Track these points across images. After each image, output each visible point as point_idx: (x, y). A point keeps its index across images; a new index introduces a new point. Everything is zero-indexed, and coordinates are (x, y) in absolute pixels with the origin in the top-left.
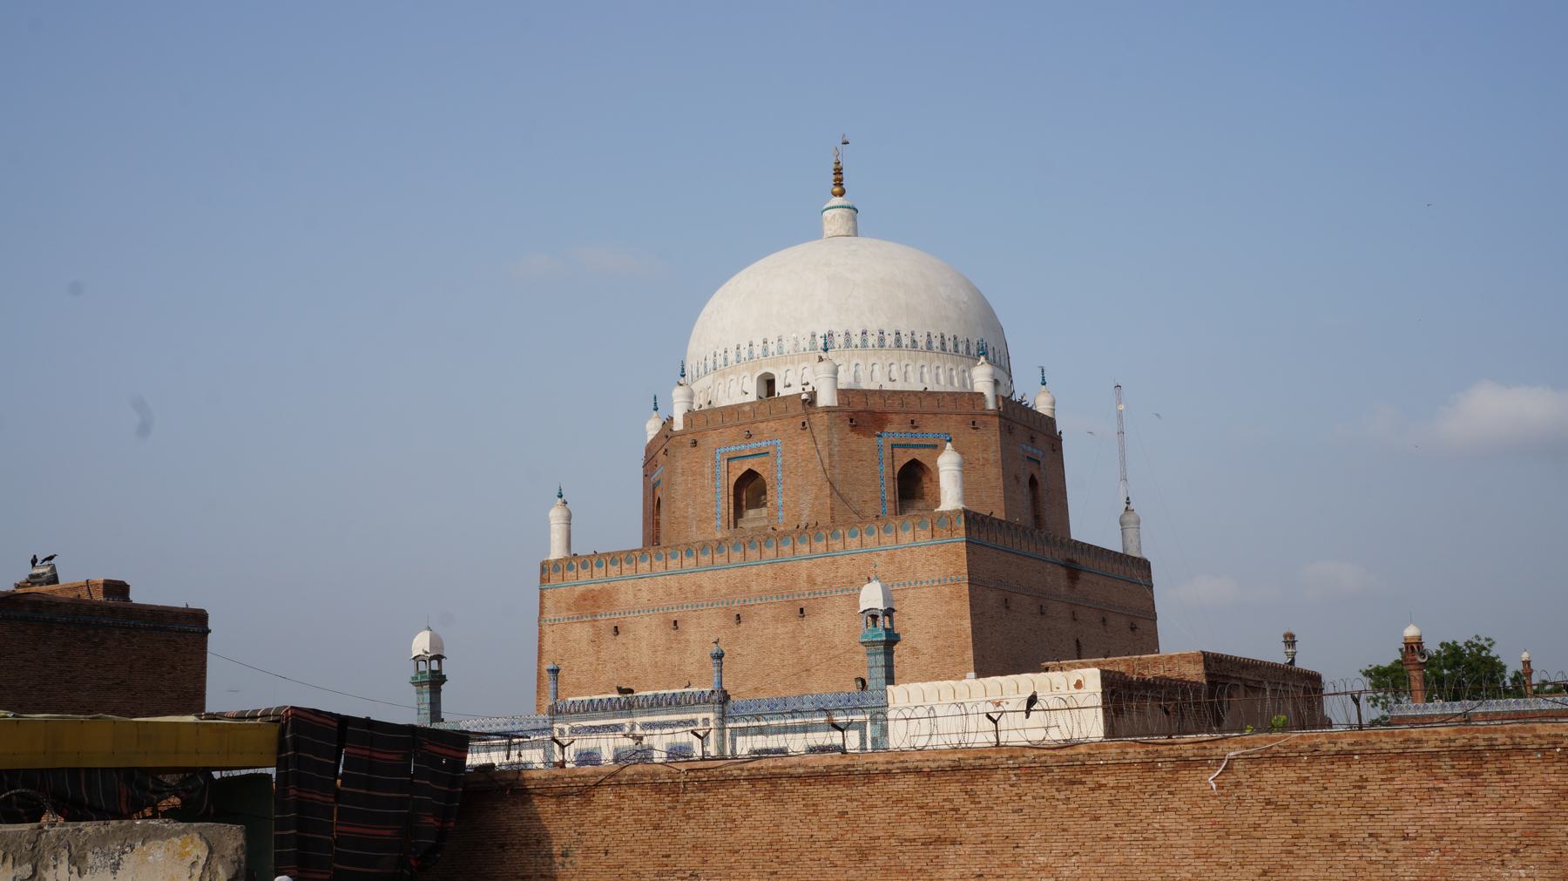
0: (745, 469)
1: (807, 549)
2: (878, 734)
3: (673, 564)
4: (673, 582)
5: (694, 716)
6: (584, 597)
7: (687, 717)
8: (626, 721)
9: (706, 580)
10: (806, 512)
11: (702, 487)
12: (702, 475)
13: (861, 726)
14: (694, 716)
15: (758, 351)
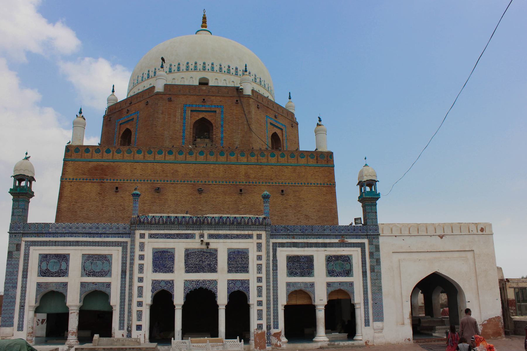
0: (201, 116)
1: (246, 159)
2: (374, 250)
3: (159, 157)
4: (158, 167)
5: (250, 232)
6: (96, 168)
7: (246, 232)
8: (197, 233)
9: (181, 169)
10: (237, 143)
11: (174, 122)
12: (175, 116)
13: (362, 246)
14: (250, 232)
15: (200, 67)
